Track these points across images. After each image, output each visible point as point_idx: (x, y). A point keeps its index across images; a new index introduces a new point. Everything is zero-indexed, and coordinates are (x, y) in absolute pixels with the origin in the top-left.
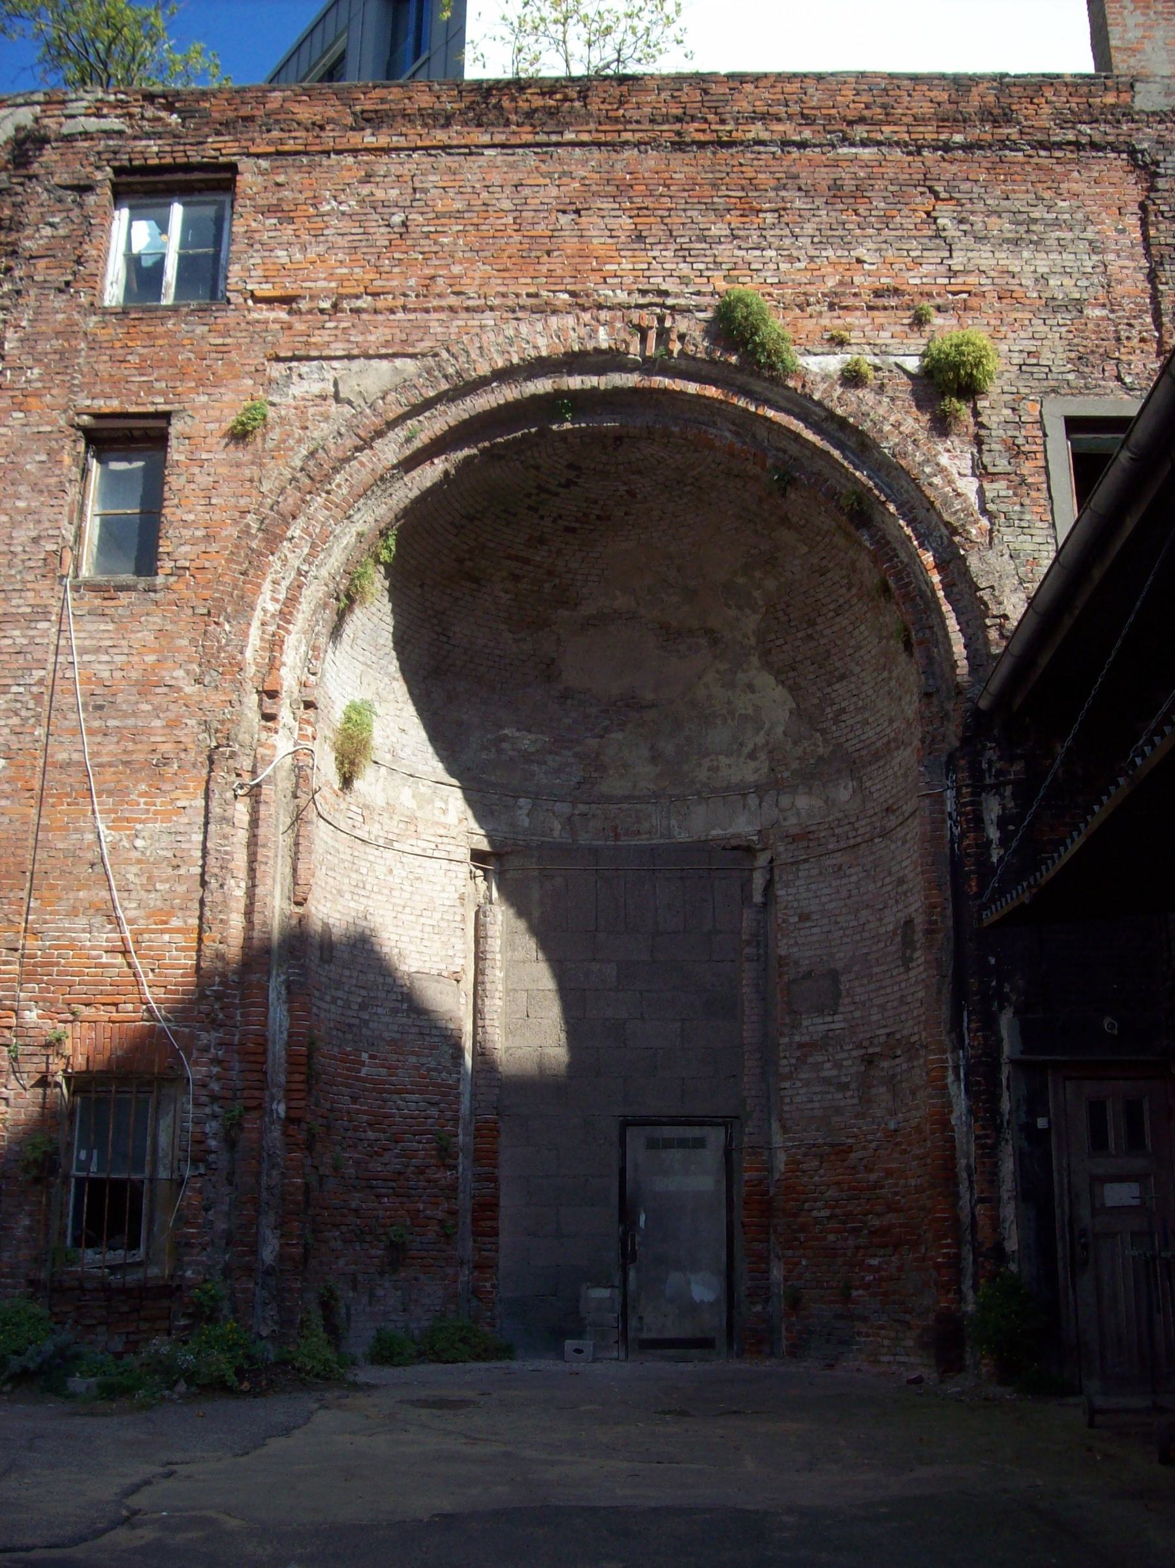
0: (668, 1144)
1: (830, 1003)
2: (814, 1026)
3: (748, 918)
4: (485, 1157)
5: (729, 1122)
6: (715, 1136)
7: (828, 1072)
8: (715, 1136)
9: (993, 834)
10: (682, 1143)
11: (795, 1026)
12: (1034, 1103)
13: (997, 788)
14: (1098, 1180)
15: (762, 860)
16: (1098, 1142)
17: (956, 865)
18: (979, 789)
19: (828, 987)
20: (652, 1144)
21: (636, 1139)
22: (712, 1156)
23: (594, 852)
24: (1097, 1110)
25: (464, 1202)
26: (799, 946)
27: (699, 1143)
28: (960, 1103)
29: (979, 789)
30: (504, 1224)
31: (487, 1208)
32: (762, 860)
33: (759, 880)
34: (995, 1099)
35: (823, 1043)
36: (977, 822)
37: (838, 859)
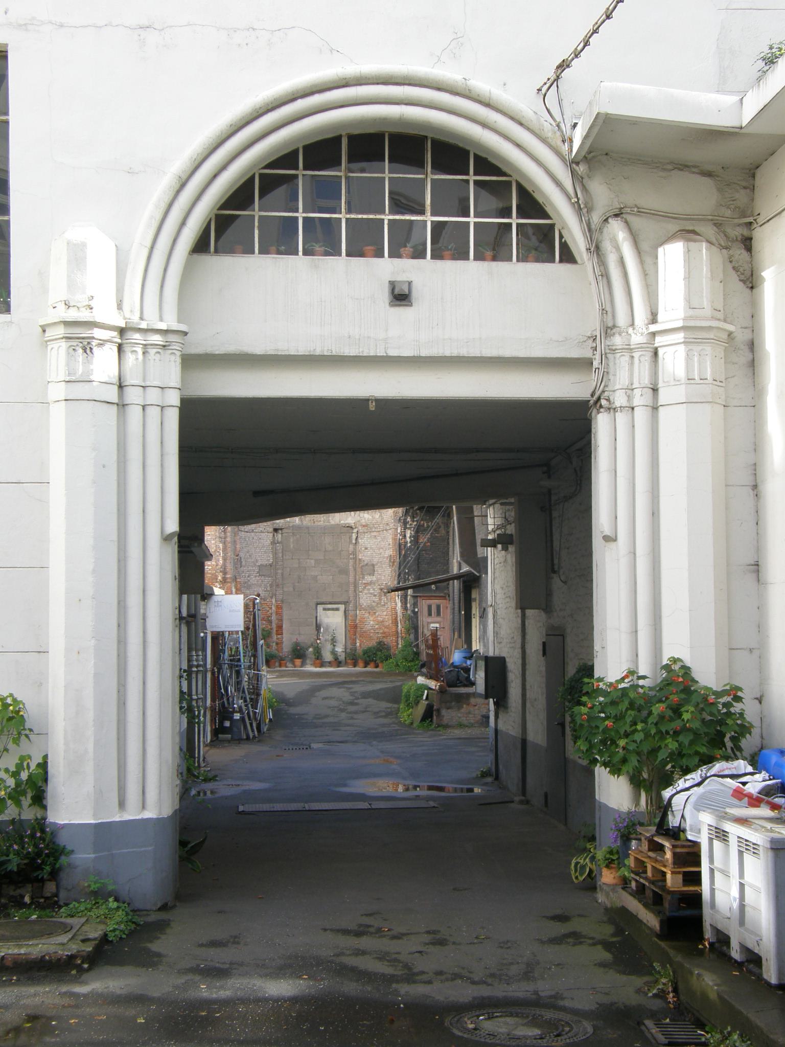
0: (329, 609)
1: (372, 573)
2: (368, 578)
3: (351, 547)
4: (279, 614)
5: (345, 603)
6: (342, 607)
7: (371, 591)
8: (342, 607)
9: (408, 540)
10: (333, 609)
11: (363, 578)
12: (415, 605)
13: (409, 528)
14: (429, 623)
15: (355, 531)
16: (430, 614)
17: (400, 545)
18: (405, 528)
19: (371, 568)
20: (324, 609)
21: (320, 608)
22: (340, 613)
23: (308, 528)
24: (430, 607)
25: (274, 626)
26: (365, 556)
27: (337, 609)
28: (399, 604)
29: (405, 528)
30: (284, 632)
31: (280, 627)
32: (355, 531)
33: (354, 536)
34: (406, 604)
35: (371, 583)
36: (405, 536)
37: (375, 534)
